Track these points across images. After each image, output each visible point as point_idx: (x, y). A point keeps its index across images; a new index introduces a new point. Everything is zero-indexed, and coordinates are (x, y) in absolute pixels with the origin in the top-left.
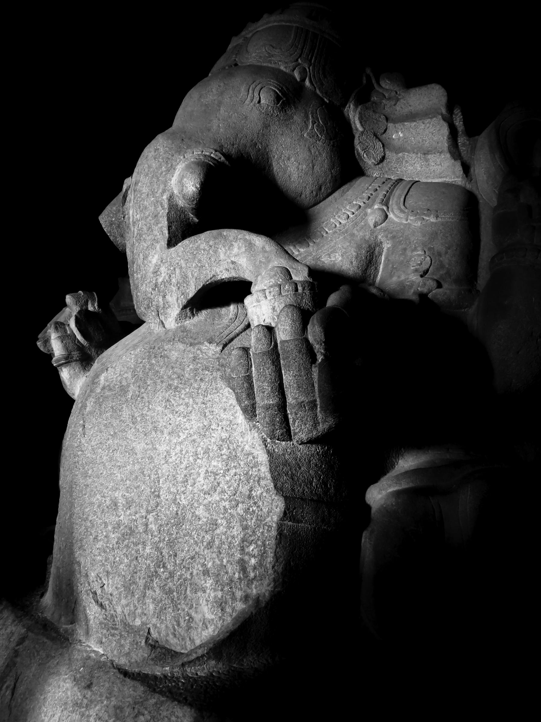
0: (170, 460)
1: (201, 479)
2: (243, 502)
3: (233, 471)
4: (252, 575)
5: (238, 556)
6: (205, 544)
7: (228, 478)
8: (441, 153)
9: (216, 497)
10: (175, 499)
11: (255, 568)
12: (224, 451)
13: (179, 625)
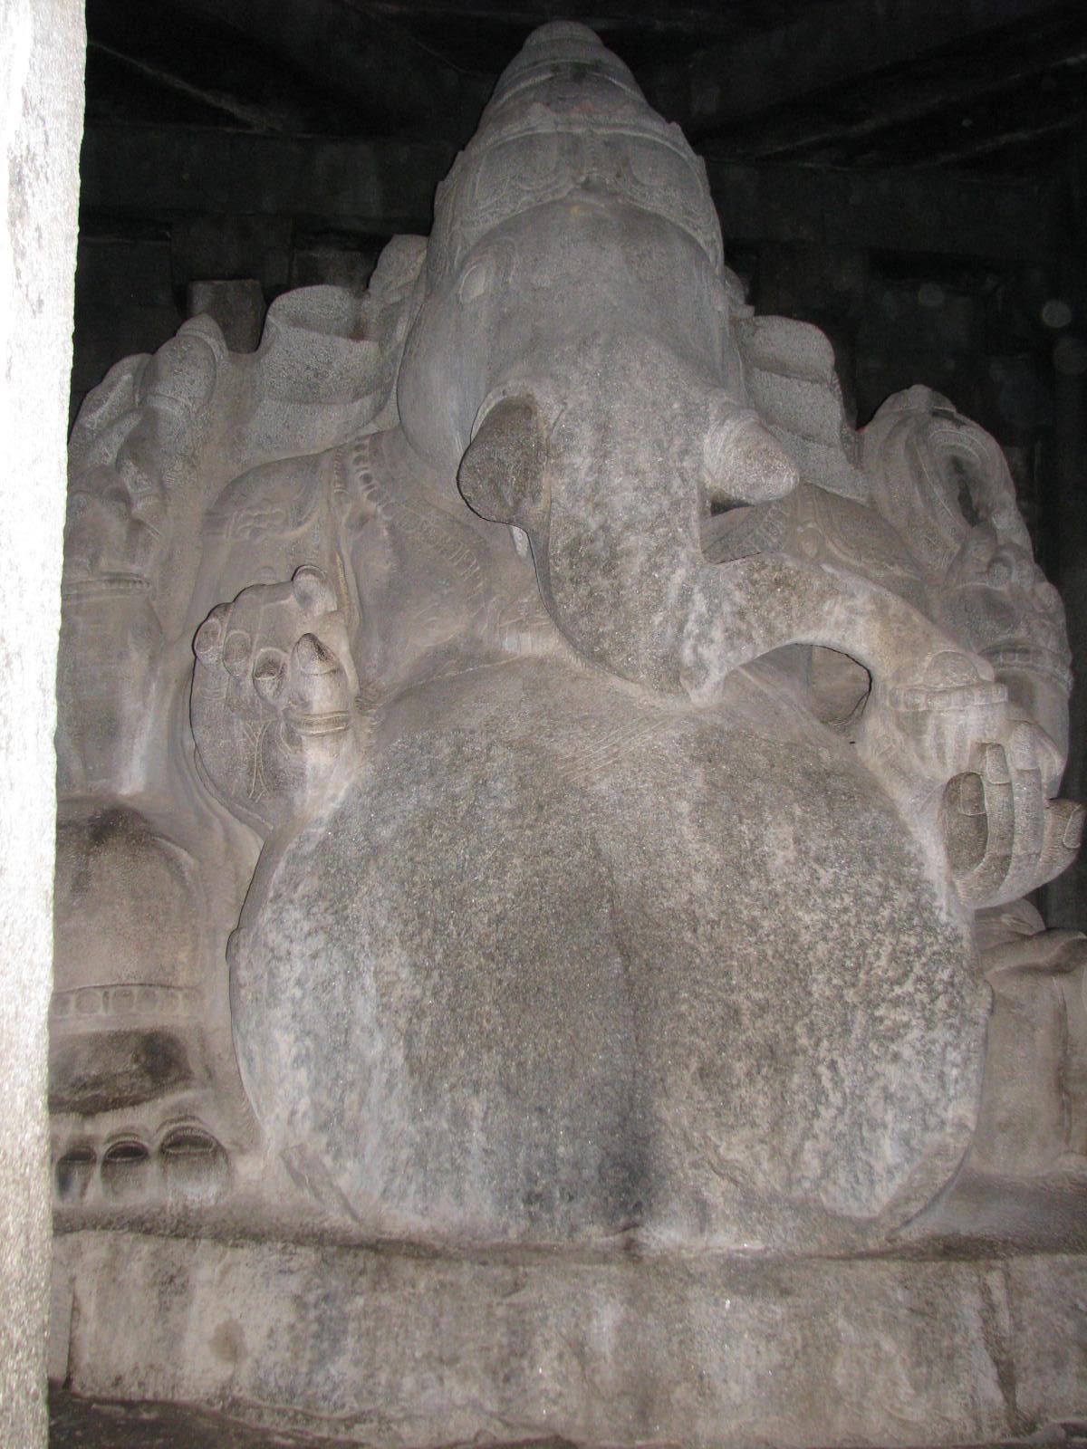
0: (830, 935)
1: (883, 962)
2: (946, 992)
6: (889, 1057)
7: (924, 959)
8: (830, 446)
9: (909, 986)
10: (842, 997)
11: (956, 1081)
12: (916, 921)
13: (857, 1182)
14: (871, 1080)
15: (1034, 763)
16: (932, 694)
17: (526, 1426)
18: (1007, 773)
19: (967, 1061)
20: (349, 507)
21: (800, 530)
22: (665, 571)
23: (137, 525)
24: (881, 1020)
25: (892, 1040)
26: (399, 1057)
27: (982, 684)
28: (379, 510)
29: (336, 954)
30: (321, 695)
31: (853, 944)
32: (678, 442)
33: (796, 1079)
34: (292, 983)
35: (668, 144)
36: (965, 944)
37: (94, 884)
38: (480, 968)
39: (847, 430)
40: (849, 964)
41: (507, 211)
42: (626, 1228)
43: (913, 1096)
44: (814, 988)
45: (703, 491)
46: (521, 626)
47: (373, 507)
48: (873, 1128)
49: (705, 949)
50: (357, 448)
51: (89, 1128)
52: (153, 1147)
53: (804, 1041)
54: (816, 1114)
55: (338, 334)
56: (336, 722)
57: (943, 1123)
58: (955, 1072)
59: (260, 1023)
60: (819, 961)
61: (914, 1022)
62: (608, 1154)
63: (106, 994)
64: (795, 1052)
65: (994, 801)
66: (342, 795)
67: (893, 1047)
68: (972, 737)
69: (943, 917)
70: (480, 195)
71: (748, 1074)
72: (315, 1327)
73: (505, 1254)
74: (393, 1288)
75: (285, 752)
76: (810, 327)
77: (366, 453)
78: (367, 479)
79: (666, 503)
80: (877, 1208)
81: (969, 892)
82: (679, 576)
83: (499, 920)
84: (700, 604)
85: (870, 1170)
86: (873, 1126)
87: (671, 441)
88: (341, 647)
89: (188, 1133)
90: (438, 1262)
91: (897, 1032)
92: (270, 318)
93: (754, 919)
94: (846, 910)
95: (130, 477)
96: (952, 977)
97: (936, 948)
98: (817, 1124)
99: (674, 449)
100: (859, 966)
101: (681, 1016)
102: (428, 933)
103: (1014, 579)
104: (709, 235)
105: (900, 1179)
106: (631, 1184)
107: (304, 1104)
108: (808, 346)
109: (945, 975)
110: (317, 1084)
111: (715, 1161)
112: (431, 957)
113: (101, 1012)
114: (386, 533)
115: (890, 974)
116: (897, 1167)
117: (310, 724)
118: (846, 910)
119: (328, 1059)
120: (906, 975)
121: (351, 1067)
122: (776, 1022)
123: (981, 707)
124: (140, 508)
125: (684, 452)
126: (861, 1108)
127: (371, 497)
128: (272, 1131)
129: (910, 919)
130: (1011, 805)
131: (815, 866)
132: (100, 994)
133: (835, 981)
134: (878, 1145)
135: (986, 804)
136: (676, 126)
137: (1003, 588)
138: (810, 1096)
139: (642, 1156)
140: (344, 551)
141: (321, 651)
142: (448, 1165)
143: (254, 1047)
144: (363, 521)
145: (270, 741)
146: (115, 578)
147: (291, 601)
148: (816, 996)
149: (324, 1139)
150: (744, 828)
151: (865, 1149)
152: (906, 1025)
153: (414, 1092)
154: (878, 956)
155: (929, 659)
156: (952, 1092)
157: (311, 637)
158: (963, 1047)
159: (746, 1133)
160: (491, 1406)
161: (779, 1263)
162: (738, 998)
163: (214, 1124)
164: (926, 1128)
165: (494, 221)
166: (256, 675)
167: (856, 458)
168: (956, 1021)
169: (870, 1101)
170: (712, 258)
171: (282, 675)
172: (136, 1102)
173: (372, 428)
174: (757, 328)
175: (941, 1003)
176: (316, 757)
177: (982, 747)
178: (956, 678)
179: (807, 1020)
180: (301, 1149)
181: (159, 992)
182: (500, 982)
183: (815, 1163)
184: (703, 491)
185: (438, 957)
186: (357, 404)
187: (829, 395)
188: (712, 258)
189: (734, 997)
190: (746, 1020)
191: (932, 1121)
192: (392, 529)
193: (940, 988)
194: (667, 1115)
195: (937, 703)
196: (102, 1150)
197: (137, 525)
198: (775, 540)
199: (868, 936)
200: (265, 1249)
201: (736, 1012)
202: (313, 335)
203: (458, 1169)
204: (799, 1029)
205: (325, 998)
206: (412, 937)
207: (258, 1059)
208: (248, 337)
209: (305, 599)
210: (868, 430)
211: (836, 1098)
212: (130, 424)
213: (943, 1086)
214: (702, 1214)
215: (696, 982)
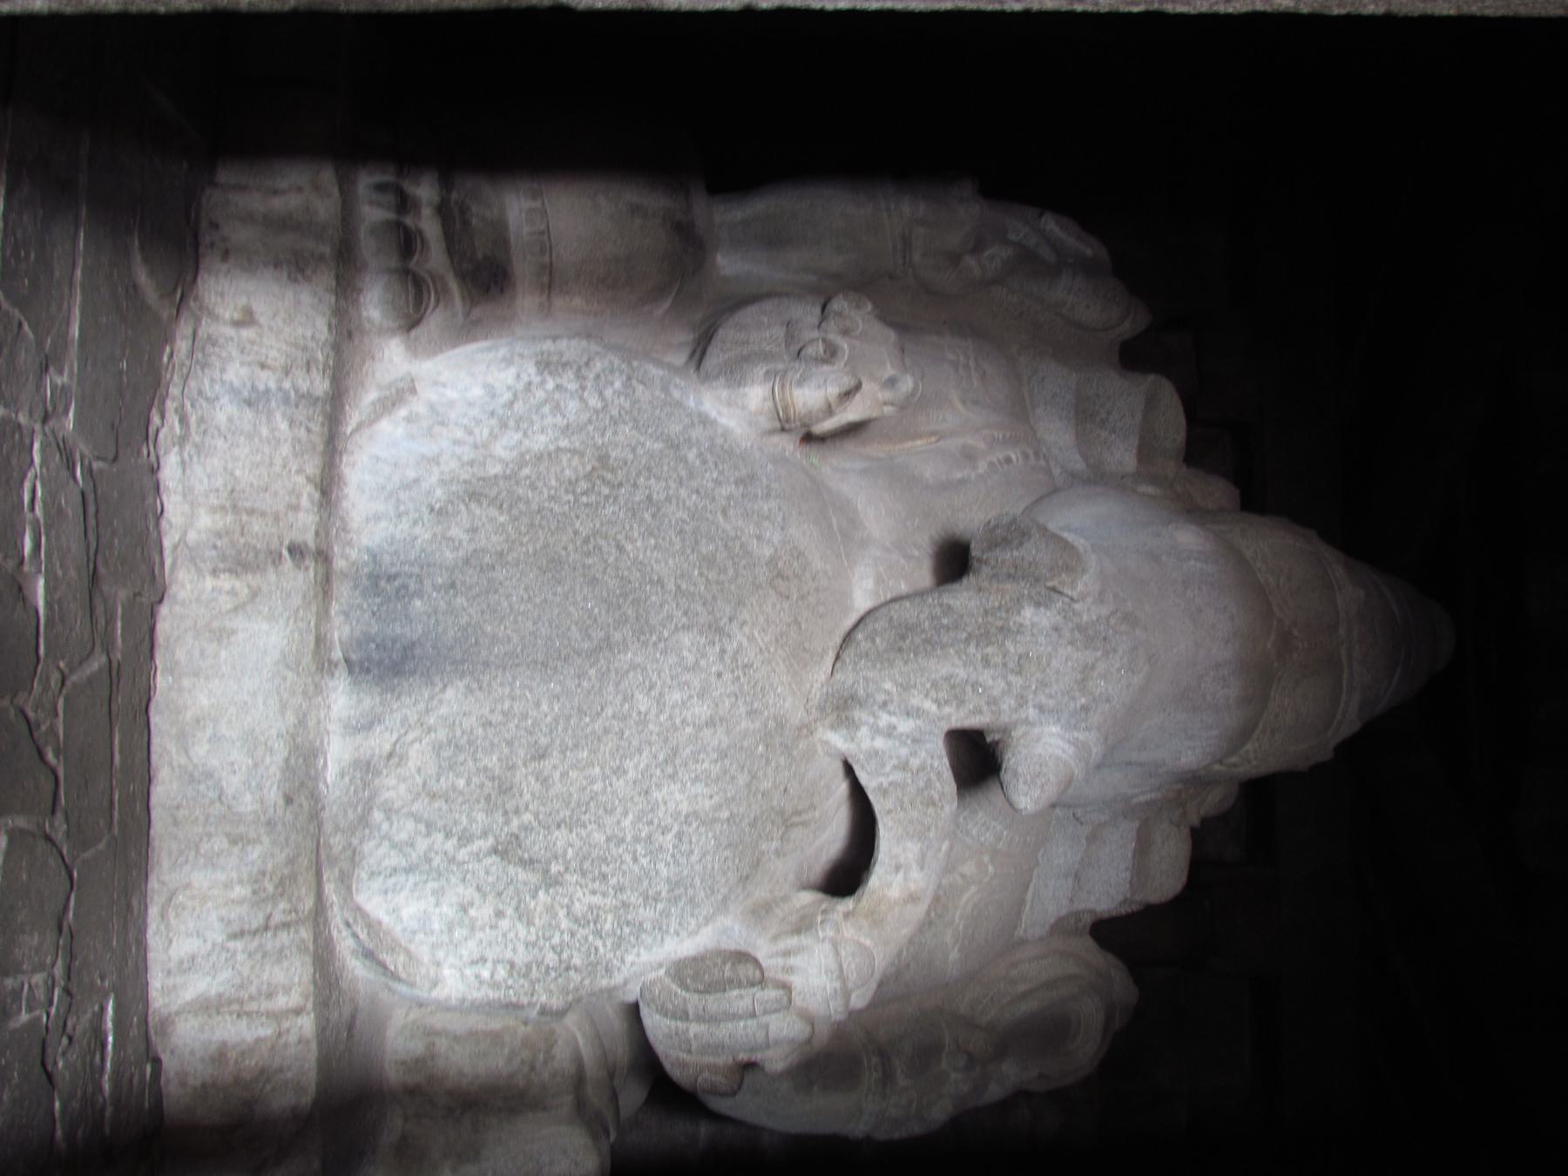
0: (612, 845)
3: (599, 943)
4: (468, 972)
5: (490, 955)
7: (591, 938)
8: (1071, 900)
9: (565, 924)
11: (477, 976)
12: (627, 930)
14: (478, 888)
15: (776, 1042)
16: (835, 945)
17: (174, 564)
18: (765, 1012)
19: (495, 985)
20: (982, 445)
21: (986, 859)
22: (933, 694)
23: (955, 259)
24: (534, 897)
25: (517, 909)
26: (495, 469)
27: (847, 994)
28: (981, 471)
29: (585, 417)
31: (604, 868)
32: (1051, 703)
33: (480, 816)
34: (559, 381)
35: (1338, 717)
36: (604, 983)
37: (638, 221)
38: (576, 533)
39: (1088, 920)
40: (587, 865)
41: (1259, 564)
42: (346, 660)
44: (564, 830)
46: (879, 580)
47: (982, 466)
48: (435, 892)
49: (598, 726)
50: (1036, 454)
51: (427, 212)
52: (412, 265)
54: (448, 835)
55: (1142, 438)
56: (785, 409)
57: (438, 964)
58: (486, 974)
59: (521, 356)
60: (589, 835)
61: (533, 930)
62: (413, 644)
63: (542, 233)
64: (506, 813)
65: (739, 999)
66: (723, 421)
67: (510, 911)
68: (796, 981)
70: (1273, 546)
71: (486, 769)
72: (261, 387)
74: (296, 455)
75: (760, 370)
76: (1184, 879)
77: (1032, 461)
78: (1008, 460)
79: (996, 692)
80: (360, 899)
81: (653, 983)
82: (930, 706)
83: (620, 548)
85: (396, 890)
86: (438, 894)
87: (1051, 696)
88: (853, 413)
89: (425, 294)
90: (317, 495)
91: (524, 916)
92: (1151, 377)
93: (625, 772)
94: (635, 860)
95: (997, 255)
96: (576, 969)
97: (601, 950)
98: (440, 837)
99: (1043, 699)
100: (584, 874)
101: (538, 705)
102: (606, 491)
103: (953, 1075)
104: (1258, 758)
105: (386, 919)
106: (387, 664)
107: (451, 394)
108: (1168, 876)
109: (577, 961)
110: (471, 404)
111: (410, 737)
112: (585, 493)
113: (526, 230)
114: (959, 475)
115: (577, 904)
116: (399, 919)
117: (783, 386)
118: (635, 860)
119: (492, 413)
120: (576, 920)
121: (486, 432)
122: (533, 795)
123: (825, 989)
124: (970, 261)
125: (1041, 708)
126: (454, 880)
127: (991, 464)
129: (628, 924)
130: (735, 1017)
131: (676, 829)
132: (543, 227)
133: (570, 851)
134: (419, 898)
135: (735, 993)
136: (1356, 727)
137: (944, 1065)
138: (465, 830)
139: (413, 673)
140: (941, 443)
141: (847, 395)
142: (402, 508)
143: (502, 352)
144: (969, 456)
145: (766, 357)
146: (906, 242)
147: (889, 371)
148: (557, 833)
150: (706, 765)
151: (416, 885)
152: (530, 923)
153: (465, 482)
154: (594, 893)
155: (868, 942)
156: (468, 972)
157: (858, 387)
158: (510, 982)
159: (431, 769)
160: (192, 536)
161: (315, 797)
162: (555, 757)
164: (434, 946)
165: (1249, 554)
167: (1060, 927)
168: (534, 973)
169: (461, 889)
170: (1234, 759)
171: (825, 361)
172: (450, 252)
173: (1057, 471)
174: (1178, 826)
175: (551, 958)
176: (756, 395)
177: (786, 987)
178: (851, 967)
179: (535, 824)
180: (413, 391)
181: (546, 279)
182: (565, 548)
183: (403, 836)
184: (1006, 730)
185: (584, 499)
186: (1078, 457)
187: (1120, 898)
188: (1234, 759)
189: (555, 754)
190: (533, 765)
192: (963, 481)
193: (565, 956)
194: (450, 693)
195: (827, 946)
196: (408, 221)
197: (955, 259)
198: (974, 832)
199: (613, 881)
200: (328, 349)
201: (542, 757)
202: (1139, 416)
203: (399, 516)
204: (527, 817)
205: (546, 409)
206: (603, 479)
207: (491, 355)
208: (1134, 357)
209: (891, 383)
210: (1090, 942)
211: (463, 854)
212: (1047, 254)
213: (473, 963)
215: (568, 718)
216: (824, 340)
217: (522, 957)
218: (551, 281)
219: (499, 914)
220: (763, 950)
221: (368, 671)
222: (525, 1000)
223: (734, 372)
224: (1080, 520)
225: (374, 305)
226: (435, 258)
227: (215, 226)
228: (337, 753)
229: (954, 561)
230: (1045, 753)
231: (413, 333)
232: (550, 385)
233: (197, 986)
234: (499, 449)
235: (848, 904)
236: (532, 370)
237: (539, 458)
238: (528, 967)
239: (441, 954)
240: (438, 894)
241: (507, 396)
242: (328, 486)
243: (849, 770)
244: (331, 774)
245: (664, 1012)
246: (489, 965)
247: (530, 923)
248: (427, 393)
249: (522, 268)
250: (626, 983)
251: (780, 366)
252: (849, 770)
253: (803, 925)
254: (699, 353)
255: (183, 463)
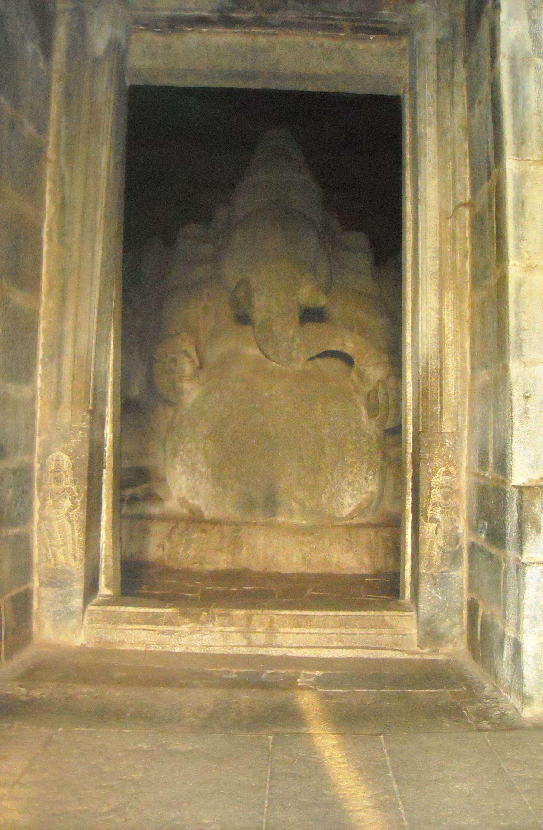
5: (365, 476)
11: (371, 480)
25: (350, 467)
26: (210, 471)
30: (187, 368)
43: (357, 483)
45: (300, 306)
53: (322, 466)
58: (371, 477)
65: (380, 397)
69: (368, 432)
73: (237, 524)
80: (344, 515)
84: (298, 341)
86: (344, 491)
88: (193, 353)
90: (218, 525)
105: (352, 508)
106: (271, 504)
107: (184, 486)
109: (368, 448)
110: (188, 480)
116: (352, 504)
128: (175, 494)
141: (188, 355)
149: (189, 495)
152: (355, 463)
163: (160, 492)
166: (170, 362)
175: (366, 457)
176: (186, 386)
177: (379, 381)
191: (364, 491)
194: (282, 485)
195: (367, 369)
214: (291, 512)
216: (170, 362)
217: (365, 466)
218: (143, 453)
219: (352, 472)
220: (368, 389)
221: (273, 510)
222: (379, 466)
223: (179, 392)
224: (231, 273)
225: (155, 510)
226: (138, 491)
227: (132, 556)
228: (298, 520)
229: (243, 319)
230: (306, 293)
231: (163, 497)
232: (182, 453)
233: (366, 560)
234: (204, 470)
235: (355, 360)
236: (177, 459)
237: (206, 457)
238: (369, 464)
239: (364, 491)
240: (344, 491)
241: (185, 468)
242: (215, 522)
243: (311, 359)
244: (305, 522)
245: (385, 422)
246: (368, 476)
247: (355, 463)
248: (184, 492)
249: (140, 463)
250: (376, 433)
251: (177, 377)
252: (311, 359)
253: (361, 375)
254: (168, 403)
255: (208, 563)
